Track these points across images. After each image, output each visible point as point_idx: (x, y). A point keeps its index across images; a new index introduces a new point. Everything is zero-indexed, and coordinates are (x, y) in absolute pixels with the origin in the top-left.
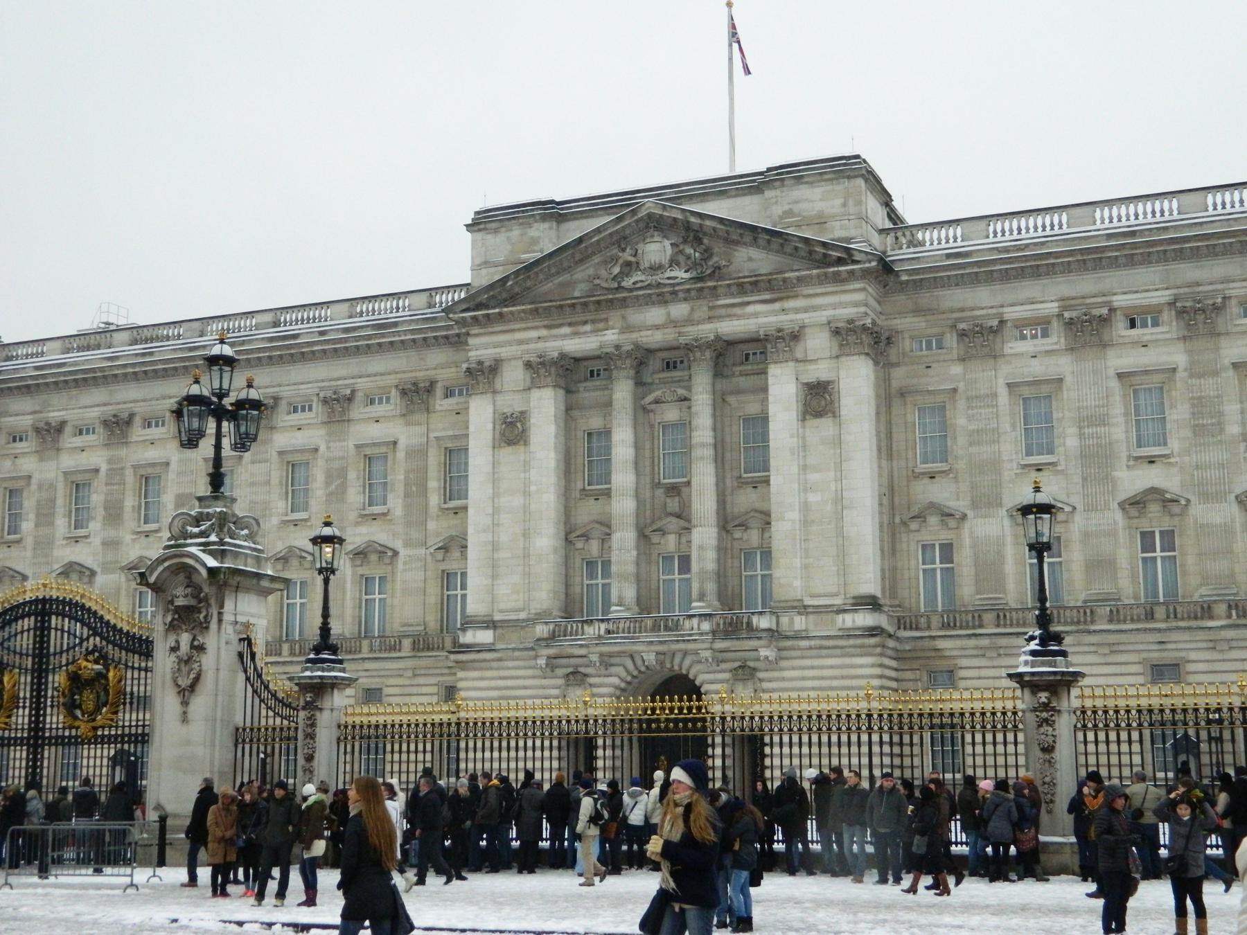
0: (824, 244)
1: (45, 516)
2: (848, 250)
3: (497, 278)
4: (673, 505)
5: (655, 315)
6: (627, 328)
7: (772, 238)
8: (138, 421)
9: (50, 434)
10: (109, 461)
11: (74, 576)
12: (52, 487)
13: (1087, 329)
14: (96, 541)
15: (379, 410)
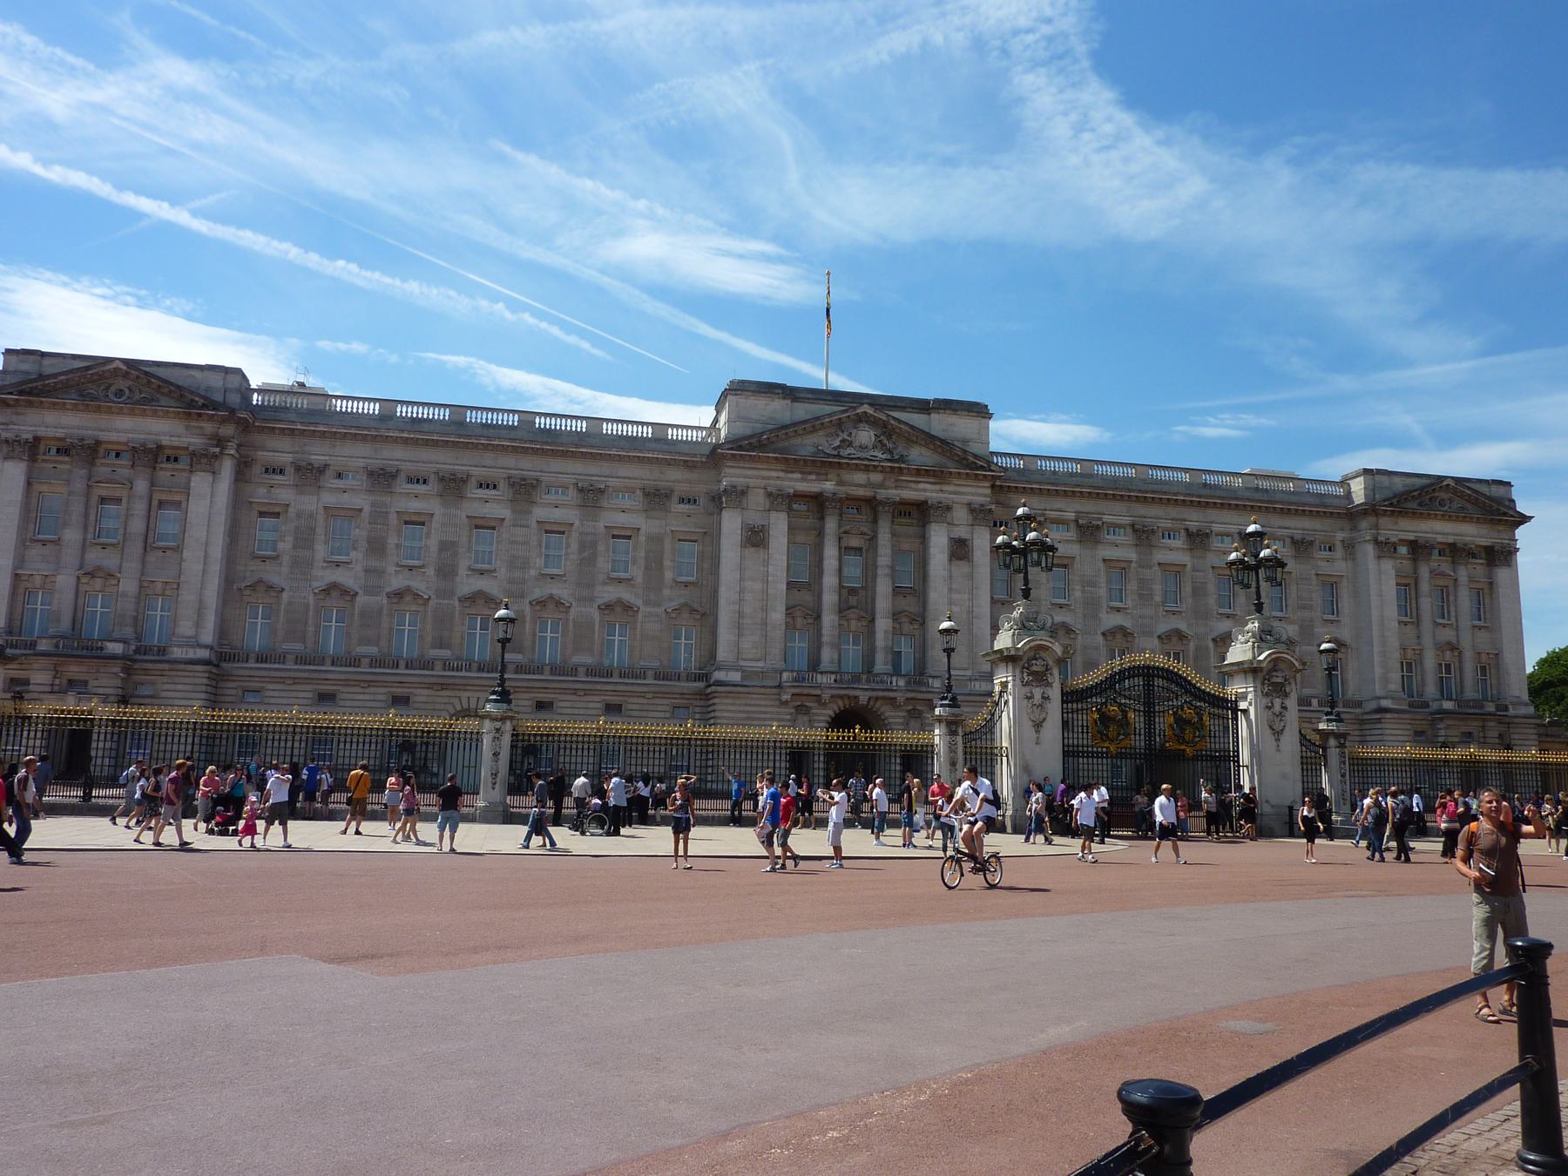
0: (976, 456)
1: (304, 539)
2: (989, 463)
3: (748, 432)
4: (853, 600)
5: (860, 477)
6: (840, 483)
7: (943, 445)
8: (403, 476)
9: (310, 474)
10: (373, 505)
11: (334, 594)
12: (311, 516)
13: (1089, 532)
14: (359, 568)
15: (627, 502)
